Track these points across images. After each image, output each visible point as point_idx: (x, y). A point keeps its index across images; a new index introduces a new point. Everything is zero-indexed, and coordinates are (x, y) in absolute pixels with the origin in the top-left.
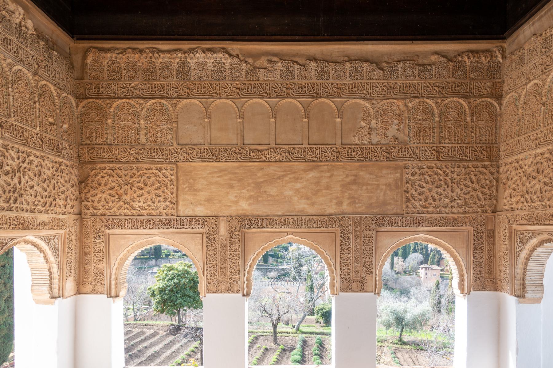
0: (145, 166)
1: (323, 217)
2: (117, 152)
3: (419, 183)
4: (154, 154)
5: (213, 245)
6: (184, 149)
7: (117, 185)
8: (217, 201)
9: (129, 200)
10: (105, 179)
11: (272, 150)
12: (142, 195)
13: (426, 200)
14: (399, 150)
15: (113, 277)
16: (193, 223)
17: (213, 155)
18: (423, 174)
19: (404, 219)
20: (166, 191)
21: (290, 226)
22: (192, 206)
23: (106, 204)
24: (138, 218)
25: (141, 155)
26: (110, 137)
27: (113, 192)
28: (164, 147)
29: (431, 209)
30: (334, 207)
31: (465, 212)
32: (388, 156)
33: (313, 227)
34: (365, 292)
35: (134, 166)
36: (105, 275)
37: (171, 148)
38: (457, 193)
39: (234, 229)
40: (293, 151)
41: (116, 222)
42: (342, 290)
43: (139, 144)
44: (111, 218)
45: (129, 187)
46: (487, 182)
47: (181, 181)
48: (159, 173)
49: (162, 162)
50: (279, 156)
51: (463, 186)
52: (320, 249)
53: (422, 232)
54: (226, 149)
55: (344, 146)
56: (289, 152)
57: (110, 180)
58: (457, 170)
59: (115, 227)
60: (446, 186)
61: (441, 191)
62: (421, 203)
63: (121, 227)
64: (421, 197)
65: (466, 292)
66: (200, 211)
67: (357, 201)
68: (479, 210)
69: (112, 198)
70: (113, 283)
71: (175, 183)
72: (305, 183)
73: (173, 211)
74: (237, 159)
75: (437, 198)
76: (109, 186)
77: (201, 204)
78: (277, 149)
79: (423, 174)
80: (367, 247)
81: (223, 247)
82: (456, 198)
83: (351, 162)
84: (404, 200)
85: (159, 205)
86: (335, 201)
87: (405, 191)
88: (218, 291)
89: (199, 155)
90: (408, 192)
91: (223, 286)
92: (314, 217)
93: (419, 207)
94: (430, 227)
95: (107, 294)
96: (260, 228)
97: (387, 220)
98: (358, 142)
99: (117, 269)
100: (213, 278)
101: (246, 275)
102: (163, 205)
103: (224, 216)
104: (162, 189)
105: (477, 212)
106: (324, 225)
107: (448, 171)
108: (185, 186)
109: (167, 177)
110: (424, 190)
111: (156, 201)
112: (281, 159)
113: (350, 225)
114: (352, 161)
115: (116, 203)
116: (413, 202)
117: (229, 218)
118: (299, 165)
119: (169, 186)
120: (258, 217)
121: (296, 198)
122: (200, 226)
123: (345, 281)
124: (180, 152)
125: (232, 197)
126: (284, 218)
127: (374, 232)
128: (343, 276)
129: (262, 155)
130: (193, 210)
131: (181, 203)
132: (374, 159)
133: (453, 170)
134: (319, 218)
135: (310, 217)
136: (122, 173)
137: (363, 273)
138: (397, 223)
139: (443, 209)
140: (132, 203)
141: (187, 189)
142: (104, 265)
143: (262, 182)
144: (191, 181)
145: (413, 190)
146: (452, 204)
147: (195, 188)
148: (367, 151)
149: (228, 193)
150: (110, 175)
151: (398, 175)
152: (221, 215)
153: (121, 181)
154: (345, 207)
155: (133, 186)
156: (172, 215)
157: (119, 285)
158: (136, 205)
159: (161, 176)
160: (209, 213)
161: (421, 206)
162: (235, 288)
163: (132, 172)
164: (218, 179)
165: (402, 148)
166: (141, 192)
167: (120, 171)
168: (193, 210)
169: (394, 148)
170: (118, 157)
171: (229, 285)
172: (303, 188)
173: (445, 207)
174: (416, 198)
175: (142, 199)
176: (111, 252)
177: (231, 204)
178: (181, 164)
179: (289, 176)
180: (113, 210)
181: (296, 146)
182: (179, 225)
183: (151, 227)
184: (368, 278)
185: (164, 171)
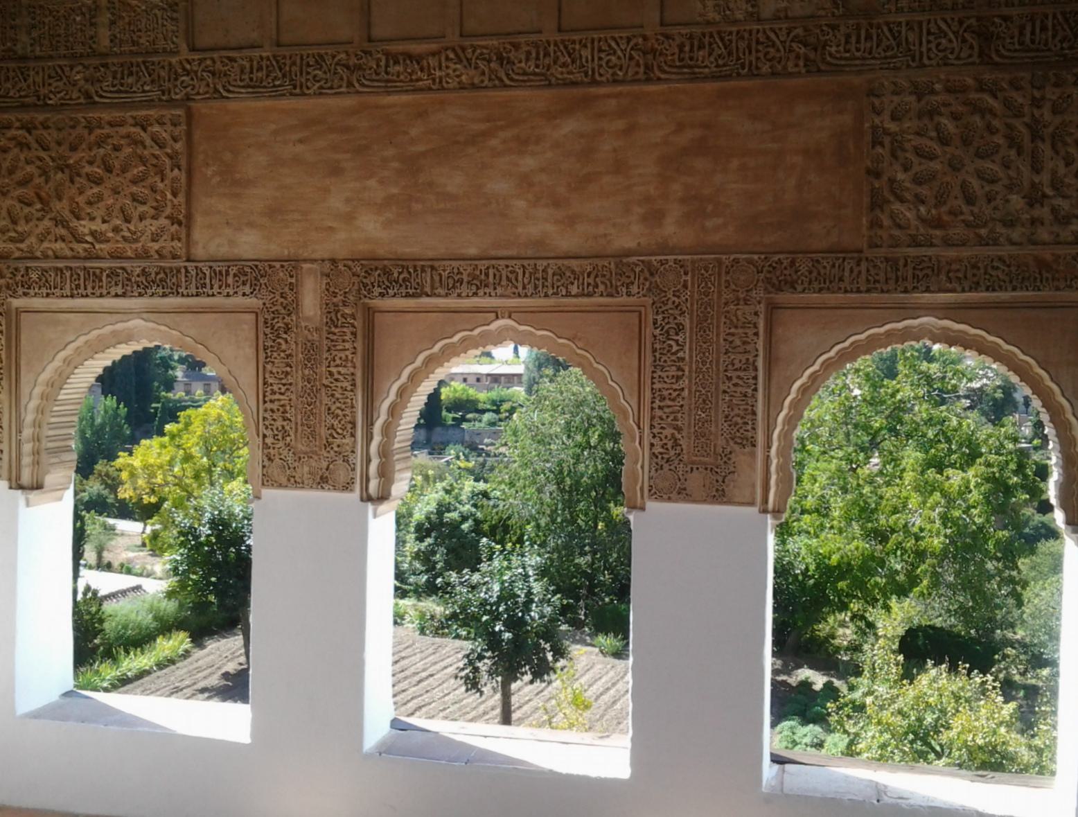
0: (106, 116)
1: (600, 263)
2: (39, 79)
3: (917, 141)
4: (130, 80)
5: (284, 347)
6: (209, 62)
7: (36, 172)
8: (297, 216)
9: (67, 214)
10: (10, 156)
11: (452, 56)
12: (100, 198)
13: (940, 200)
14: (848, 37)
15: (27, 432)
16: (230, 280)
17: (284, 76)
18: (932, 113)
20: (161, 185)
21: (499, 291)
22: (228, 231)
23: (11, 226)
24: (88, 264)
25: (98, 85)
26: (24, 38)
27: (28, 192)
28: (155, 59)
29: (958, 231)
30: (636, 228)
32: (812, 55)
33: (568, 295)
34: (730, 502)
35: (80, 115)
37: (174, 60)
38: (1054, 173)
39: (340, 298)
40: (512, 55)
41: (34, 276)
42: (658, 493)
43: (94, 54)
44: (21, 265)
45: (66, 176)
47: (201, 157)
48: (142, 134)
49: (149, 104)
50: (472, 72)
52: (596, 365)
53: (931, 309)
54: (321, 56)
55: (669, 30)
56: (500, 59)
57: (22, 157)
58: (1051, 94)
59: (32, 292)
60: (1013, 153)
62: (922, 209)
63: (44, 291)
64: (924, 191)
66: (250, 244)
67: (710, 208)
69: (27, 210)
70: (27, 448)
71: (183, 163)
72: (549, 155)
73: (177, 244)
74: (350, 84)
75: (979, 193)
76: (19, 175)
77: (251, 225)
78: (463, 49)
79: (932, 113)
80: (739, 359)
81: (311, 351)
82: (1049, 192)
83: (691, 80)
84: (866, 200)
85: (141, 226)
86: (639, 210)
87: (869, 172)
88: (294, 482)
89: (246, 77)
90: (878, 175)
91: (306, 469)
92: (574, 263)
93: (914, 222)
95: (10, 480)
96: (413, 296)
97: (804, 270)
98: (712, 15)
99: (40, 410)
100: (281, 444)
101: (377, 439)
102: (151, 226)
103: (313, 261)
104: (150, 181)
106: (602, 288)
107: (1020, 100)
108: (209, 173)
109: (162, 146)
110: (935, 165)
111: (136, 215)
112: (476, 81)
113: (685, 286)
114: (694, 78)
115: (34, 222)
116: (897, 206)
117: (328, 265)
118: (535, 99)
119: (168, 170)
120: (410, 264)
121: (521, 204)
122: (247, 289)
123: (666, 466)
124: (196, 72)
125: (336, 202)
126: (483, 265)
127: (761, 308)
128: (658, 450)
129: (422, 70)
130: (232, 243)
131: (199, 220)
132: (765, 68)
133: (1037, 94)
134: (587, 265)
135: (560, 262)
136: (50, 136)
137: (721, 442)
138: (841, 280)
139: (1000, 229)
140: (74, 223)
141: (218, 179)
143: (423, 154)
144: (228, 156)
145: (897, 167)
146: (1037, 212)
147: (238, 176)
148: (742, 45)
149: (326, 190)
150: (23, 145)
151: (847, 119)
152: (306, 254)
153: (48, 159)
154: (671, 230)
155: (79, 175)
156: (174, 257)
157: (44, 456)
158: (84, 227)
159: (148, 142)
160: (274, 249)
161: (923, 221)
162: (341, 475)
163: (75, 133)
164: (300, 148)
165: (858, 27)
166: (96, 190)
167: (45, 133)
168: (232, 243)
169: (834, 27)
170: (44, 91)
171: (325, 464)
172: (542, 170)
173: (1010, 223)
174: (908, 196)
175: (99, 212)
176: (23, 363)
177: (334, 225)
178: (200, 107)
179: (502, 134)
180: (27, 242)
181: (522, 39)
182: (193, 285)
183: (120, 292)
184: (740, 457)
185: (156, 128)
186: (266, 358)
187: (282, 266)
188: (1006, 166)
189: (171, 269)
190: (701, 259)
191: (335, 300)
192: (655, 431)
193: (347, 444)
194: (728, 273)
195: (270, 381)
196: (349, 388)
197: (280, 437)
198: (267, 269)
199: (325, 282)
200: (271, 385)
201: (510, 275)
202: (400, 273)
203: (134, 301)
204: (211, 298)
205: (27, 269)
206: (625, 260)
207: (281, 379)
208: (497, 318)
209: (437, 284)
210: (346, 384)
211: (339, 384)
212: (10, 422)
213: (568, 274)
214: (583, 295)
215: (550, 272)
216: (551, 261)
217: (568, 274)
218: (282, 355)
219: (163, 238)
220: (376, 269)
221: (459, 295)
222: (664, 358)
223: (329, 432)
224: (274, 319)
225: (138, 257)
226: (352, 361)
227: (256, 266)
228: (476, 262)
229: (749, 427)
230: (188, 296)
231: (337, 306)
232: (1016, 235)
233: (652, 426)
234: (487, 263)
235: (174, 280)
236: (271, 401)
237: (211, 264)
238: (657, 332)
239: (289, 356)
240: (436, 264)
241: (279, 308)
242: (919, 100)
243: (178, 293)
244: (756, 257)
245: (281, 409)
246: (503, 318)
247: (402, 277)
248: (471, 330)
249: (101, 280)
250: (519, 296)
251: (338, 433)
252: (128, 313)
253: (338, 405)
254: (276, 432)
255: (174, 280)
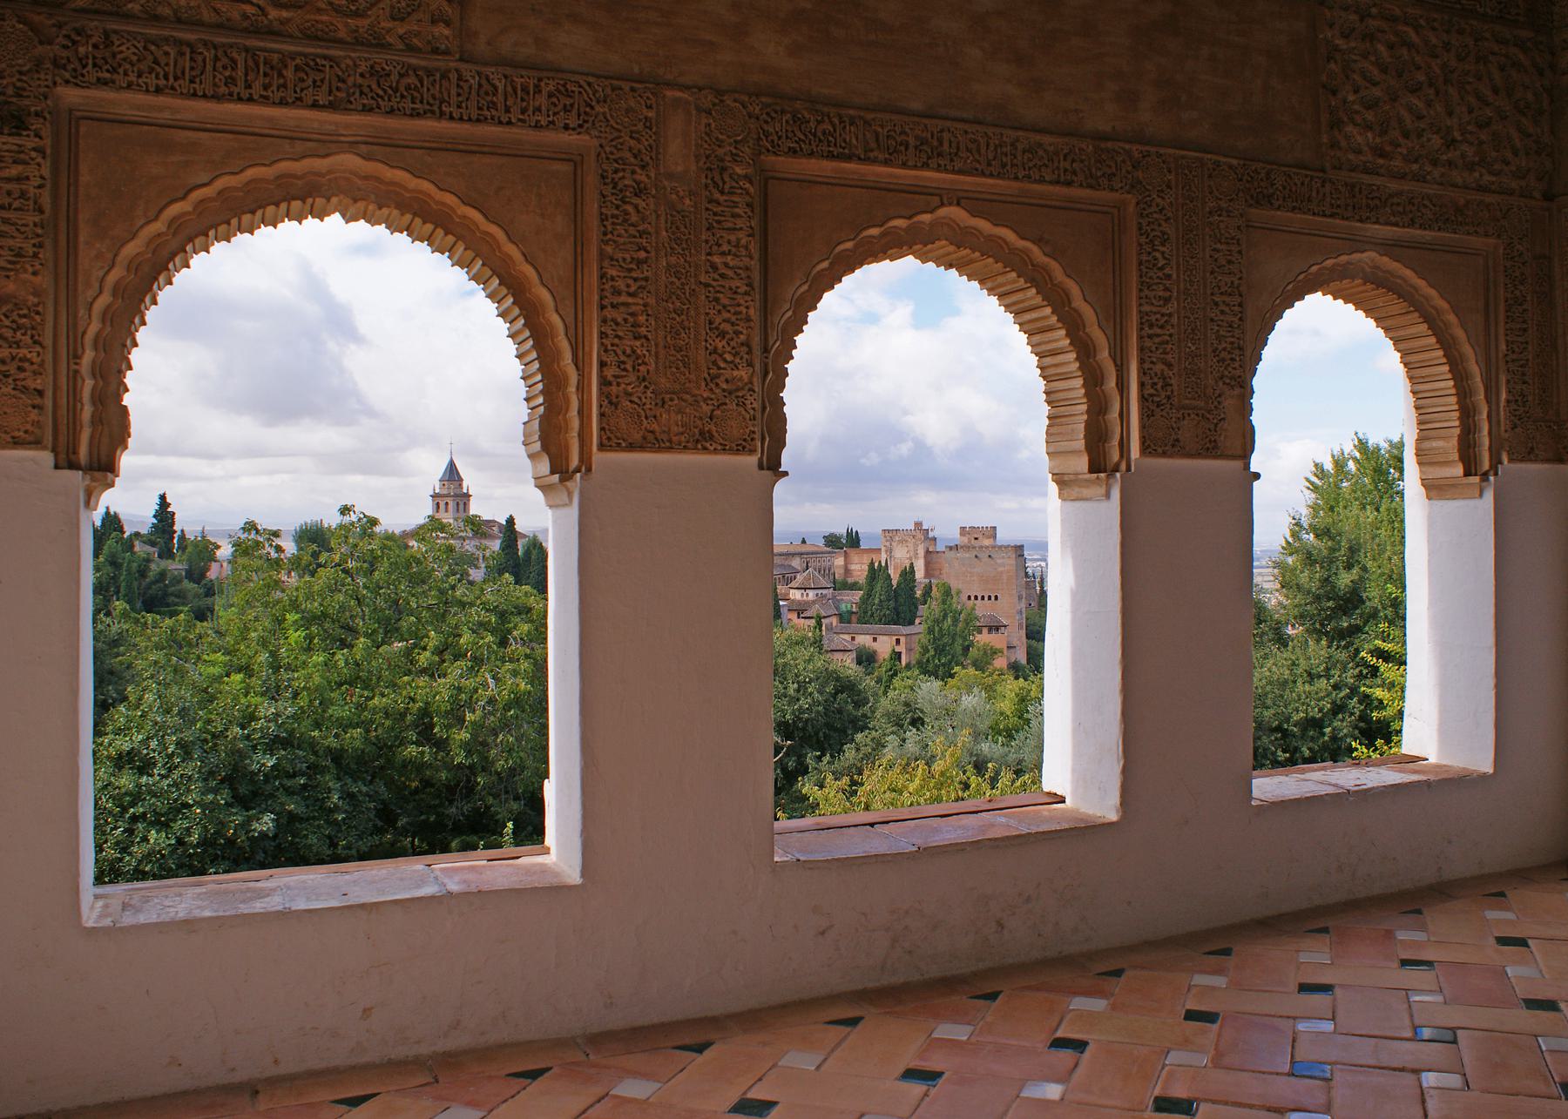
5: (634, 218)
16: (542, 100)
19: (1328, 185)
21: (958, 165)
29: (1397, 163)
31: (1482, 189)
33: (1041, 181)
36: (48, 341)
41: (127, 50)
46: (1530, 97)
51: (1472, 100)
60: (1432, 91)
61: (1421, 105)
63: (152, 81)
64: (1369, 116)
65: (1486, 466)
68: (1514, 185)
82: (1457, 135)
90: (1334, 93)
92: (1047, 139)
94: (1396, 225)
105: (1511, 193)
107: (1434, 41)
110: (1377, 92)
113: (1169, 187)
116: (1350, 129)
142: (44, 281)
171: (706, 409)
184: (1229, 403)
186: (605, 234)
187: (633, 89)
188: (1429, 104)
189: (430, 73)
190: (1183, 157)
191: (720, 152)
192: (1146, 366)
193: (741, 379)
194: (1210, 176)
195: (613, 272)
196: (744, 289)
197: (629, 367)
198: (608, 91)
199: (704, 121)
200: (613, 279)
201: (971, 146)
202: (819, 122)
203: (354, 118)
204: (507, 129)
205: (106, 34)
206: (1103, 145)
207: (630, 270)
208: (943, 205)
209: (873, 145)
210: (735, 283)
211: (727, 283)
212: (55, 336)
213: (1041, 153)
214: (1058, 182)
215: (1020, 146)
216: (1020, 133)
217: (1041, 153)
218: (632, 230)
219: (415, 16)
220: (783, 112)
221: (904, 165)
222: (1151, 274)
223: (714, 357)
224: (616, 172)
225: (358, 42)
226: (746, 248)
227: (589, 84)
228: (926, 121)
229: (1237, 365)
230: (461, 119)
231: (722, 160)
232: (1436, 173)
233: (1141, 361)
234: (941, 123)
235: (435, 91)
236: (613, 306)
237: (509, 71)
238: (1143, 240)
239: (641, 234)
240: (870, 116)
241: (628, 155)
242: (1362, 20)
243: (442, 114)
244: (1235, 162)
245: (631, 320)
246: (950, 204)
247: (821, 128)
248: (910, 218)
249: (280, 75)
250: (983, 174)
251: (725, 361)
252: (328, 144)
253: (726, 315)
254: (623, 358)
255: (435, 91)
